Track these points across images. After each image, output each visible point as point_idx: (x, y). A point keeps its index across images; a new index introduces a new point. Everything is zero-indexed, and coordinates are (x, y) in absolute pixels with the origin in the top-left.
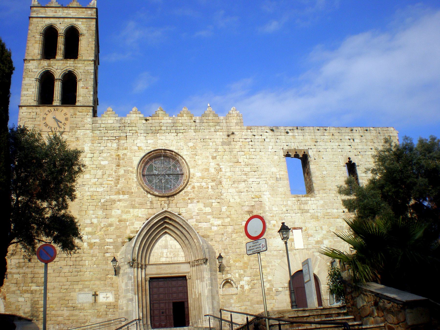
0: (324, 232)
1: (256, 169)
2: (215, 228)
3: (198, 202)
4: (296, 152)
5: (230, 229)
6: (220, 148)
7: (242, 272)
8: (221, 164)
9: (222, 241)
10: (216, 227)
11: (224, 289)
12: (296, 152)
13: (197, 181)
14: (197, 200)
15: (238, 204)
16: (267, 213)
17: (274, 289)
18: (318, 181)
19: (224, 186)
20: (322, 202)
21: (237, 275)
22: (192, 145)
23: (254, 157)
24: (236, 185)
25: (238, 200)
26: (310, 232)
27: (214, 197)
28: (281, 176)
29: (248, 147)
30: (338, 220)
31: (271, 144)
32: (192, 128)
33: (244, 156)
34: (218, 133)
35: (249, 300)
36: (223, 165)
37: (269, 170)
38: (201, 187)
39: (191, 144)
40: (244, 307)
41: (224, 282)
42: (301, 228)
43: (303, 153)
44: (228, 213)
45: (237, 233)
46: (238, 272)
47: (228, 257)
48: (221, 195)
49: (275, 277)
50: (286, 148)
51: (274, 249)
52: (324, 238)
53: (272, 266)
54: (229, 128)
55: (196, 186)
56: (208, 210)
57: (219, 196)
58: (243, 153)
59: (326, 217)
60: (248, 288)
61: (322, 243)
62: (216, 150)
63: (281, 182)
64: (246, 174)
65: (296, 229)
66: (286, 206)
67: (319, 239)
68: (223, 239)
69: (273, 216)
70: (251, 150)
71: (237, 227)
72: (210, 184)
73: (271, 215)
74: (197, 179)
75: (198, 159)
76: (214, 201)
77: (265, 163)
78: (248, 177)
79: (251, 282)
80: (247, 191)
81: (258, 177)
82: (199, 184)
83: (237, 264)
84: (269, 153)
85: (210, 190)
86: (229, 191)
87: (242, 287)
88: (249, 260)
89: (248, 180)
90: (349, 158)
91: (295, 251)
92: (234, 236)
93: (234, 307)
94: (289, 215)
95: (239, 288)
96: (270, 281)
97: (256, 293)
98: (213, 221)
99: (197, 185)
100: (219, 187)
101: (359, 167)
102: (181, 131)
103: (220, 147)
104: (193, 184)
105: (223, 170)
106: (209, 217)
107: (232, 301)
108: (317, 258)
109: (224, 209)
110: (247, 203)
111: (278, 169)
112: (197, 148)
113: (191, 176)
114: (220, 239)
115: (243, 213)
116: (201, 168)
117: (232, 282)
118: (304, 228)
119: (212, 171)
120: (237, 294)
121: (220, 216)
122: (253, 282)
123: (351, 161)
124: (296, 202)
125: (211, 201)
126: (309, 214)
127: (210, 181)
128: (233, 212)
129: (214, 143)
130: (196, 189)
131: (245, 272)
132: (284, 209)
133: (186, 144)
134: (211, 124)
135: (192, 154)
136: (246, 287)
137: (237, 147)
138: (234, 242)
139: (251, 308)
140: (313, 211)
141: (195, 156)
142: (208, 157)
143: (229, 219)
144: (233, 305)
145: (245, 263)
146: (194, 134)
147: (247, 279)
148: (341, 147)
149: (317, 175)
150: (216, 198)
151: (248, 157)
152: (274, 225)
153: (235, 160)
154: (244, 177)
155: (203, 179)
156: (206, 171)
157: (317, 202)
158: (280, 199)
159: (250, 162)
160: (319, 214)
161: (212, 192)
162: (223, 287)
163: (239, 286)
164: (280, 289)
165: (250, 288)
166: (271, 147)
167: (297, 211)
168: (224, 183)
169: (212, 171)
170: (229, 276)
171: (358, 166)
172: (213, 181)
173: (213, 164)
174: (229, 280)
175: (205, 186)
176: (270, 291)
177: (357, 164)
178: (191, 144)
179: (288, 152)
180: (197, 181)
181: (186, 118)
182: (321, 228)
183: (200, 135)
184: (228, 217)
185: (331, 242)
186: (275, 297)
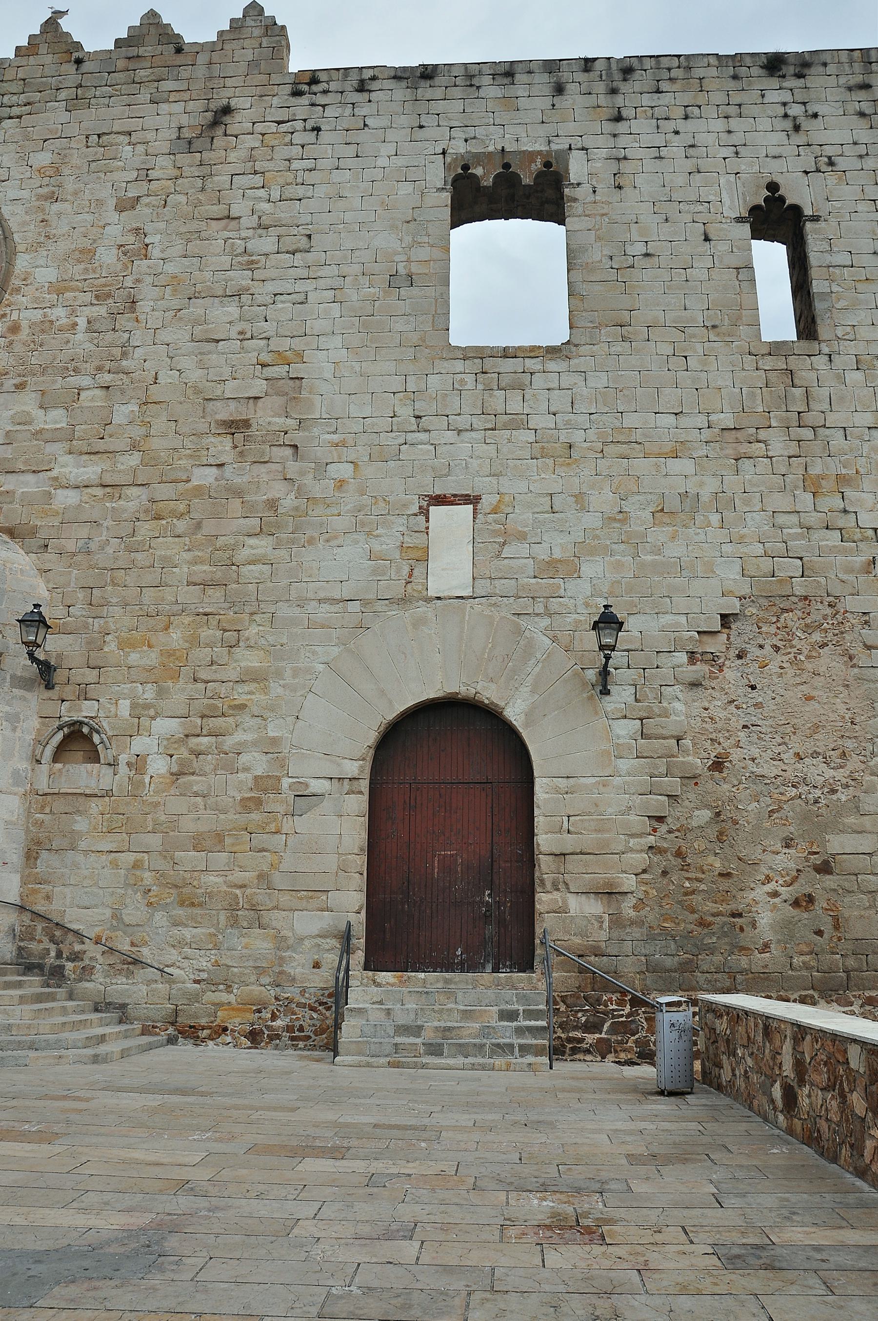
0: (592, 520)
1: (303, 243)
2: (66, 498)
3: (20, 387)
4: (507, 166)
5: (134, 500)
6: (163, 167)
7: (149, 693)
8: (148, 228)
9: (89, 553)
10: (71, 493)
11: (59, 766)
12: (507, 166)
13: (36, 299)
14: (18, 380)
15: (190, 392)
16: (316, 431)
17: (286, 782)
18: (597, 287)
19: (142, 317)
20: (599, 381)
21: (124, 708)
22: (47, 162)
23: (300, 191)
24: (197, 308)
25: (195, 375)
26: (521, 518)
27: (89, 367)
28: (415, 268)
29: (283, 152)
30: (675, 466)
31: (391, 135)
32: (63, 95)
33: (262, 193)
34: (164, 107)
35: (156, 823)
36: (157, 232)
37: (361, 244)
38: (46, 325)
39: (43, 159)
40: (131, 857)
41: (60, 736)
42: (472, 500)
43: (538, 165)
44: (137, 432)
45: (158, 518)
46: (134, 698)
47: (97, 624)
48: (124, 354)
49: (300, 723)
50: (459, 147)
51: (322, 595)
52: (586, 548)
53: (296, 673)
54: (216, 83)
55: (24, 324)
56: (57, 419)
57: (114, 362)
58: (258, 180)
59: (610, 449)
60: (163, 770)
61: (575, 573)
62: (145, 175)
63: (414, 291)
64: (251, 266)
65: (452, 503)
66: (413, 396)
67: (557, 554)
68: (93, 546)
69: (343, 444)
70: (296, 165)
71: (164, 491)
72: (87, 311)
73: (335, 437)
74: (37, 294)
75: (59, 215)
76: (86, 381)
77: (349, 217)
78: (258, 274)
79: (181, 741)
80: (241, 333)
81: (304, 273)
82: (38, 315)
83: (134, 658)
84: (378, 174)
85: (80, 336)
86: (164, 336)
87: (139, 764)
88: (194, 641)
89: (257, 287)
90: (773, 187)
91: (422, 609)
92: (145, 529)
93: (86, 852)
94: (423, 436)
95: (123, 769)
96: (275, 741)
97: (196, 795)
98: (70, 468)
99: (29, 317)
100: (124, 321)
101: (822, 224)
102: (16, 111)
103: (164, 162)
104: (15, 316)
105: (155, 252)
106: (50, 448)
107: (81, 824)
108: (530, 644)
109: (122, 413)
110: (230, 384)
111: (408, 239)
112: (66, 171)
113: (15, 282)
114: (81, 543)
115: (202, 427)
116: (63, 246)
117: (96, 738)
118: (487, 502)
119: (108, 256)
120: (109, 793)
121: (101, 446)
122: (194, 741)
123: (782, 199)
124: (470, 379)
125: (75, 381)
126: (530, 436)
127: (88, 297)
128: (160, 424)
129: (140, 148)
130: (24, 334)
131: (161, 693)
132: (405, 412)
133: (24, 158)
134: (143, 73)
135: (40, 197)
136: (158, 766)
137: (233, 156)
138: (139, 556)
139: (162, 864)
140: (548, 422)
141: (47, 204)
142: (100, 203)
143: (134, 460)
144: (82, 845)
145: (170, 654)
146: (65, 117)
147: (166, 726)
148: (736, 139)
149: (597, 257)
150: (99, 369)
151: (276, 194)
152: (341, 484)
153: (217, 210)
154: (241, 278)
155: (60, 292)
156: (79, 261)
157: (578, 379)
158: (391, 367)
159: (284, 211)
160: (578, 437)
161: (88, 345)
162: (56, 758)
163: (123, 758)
164: (317, 786)
165: (175, 769)
166: (391, 149)
167: (462, 422)
168: (144, 306)
169: (108, 256)
170: (86, 710)
171: (815, 219)
172: (101, 297)
173: (116, 228)
174: (85, 730)
175: (64, 321)
176: (265, 791)
177: (808, 212)
178: (43, 159)
179: (465, 167)
180: (36, 299)
181: (48, 59)
182: (579, 498)
183: (90, 119)
184: (134, 447)
185: (619, 566)
186: (287, 825)
